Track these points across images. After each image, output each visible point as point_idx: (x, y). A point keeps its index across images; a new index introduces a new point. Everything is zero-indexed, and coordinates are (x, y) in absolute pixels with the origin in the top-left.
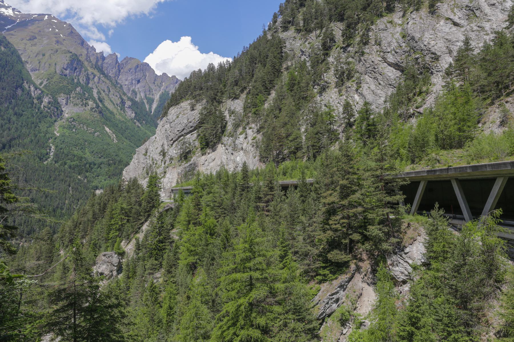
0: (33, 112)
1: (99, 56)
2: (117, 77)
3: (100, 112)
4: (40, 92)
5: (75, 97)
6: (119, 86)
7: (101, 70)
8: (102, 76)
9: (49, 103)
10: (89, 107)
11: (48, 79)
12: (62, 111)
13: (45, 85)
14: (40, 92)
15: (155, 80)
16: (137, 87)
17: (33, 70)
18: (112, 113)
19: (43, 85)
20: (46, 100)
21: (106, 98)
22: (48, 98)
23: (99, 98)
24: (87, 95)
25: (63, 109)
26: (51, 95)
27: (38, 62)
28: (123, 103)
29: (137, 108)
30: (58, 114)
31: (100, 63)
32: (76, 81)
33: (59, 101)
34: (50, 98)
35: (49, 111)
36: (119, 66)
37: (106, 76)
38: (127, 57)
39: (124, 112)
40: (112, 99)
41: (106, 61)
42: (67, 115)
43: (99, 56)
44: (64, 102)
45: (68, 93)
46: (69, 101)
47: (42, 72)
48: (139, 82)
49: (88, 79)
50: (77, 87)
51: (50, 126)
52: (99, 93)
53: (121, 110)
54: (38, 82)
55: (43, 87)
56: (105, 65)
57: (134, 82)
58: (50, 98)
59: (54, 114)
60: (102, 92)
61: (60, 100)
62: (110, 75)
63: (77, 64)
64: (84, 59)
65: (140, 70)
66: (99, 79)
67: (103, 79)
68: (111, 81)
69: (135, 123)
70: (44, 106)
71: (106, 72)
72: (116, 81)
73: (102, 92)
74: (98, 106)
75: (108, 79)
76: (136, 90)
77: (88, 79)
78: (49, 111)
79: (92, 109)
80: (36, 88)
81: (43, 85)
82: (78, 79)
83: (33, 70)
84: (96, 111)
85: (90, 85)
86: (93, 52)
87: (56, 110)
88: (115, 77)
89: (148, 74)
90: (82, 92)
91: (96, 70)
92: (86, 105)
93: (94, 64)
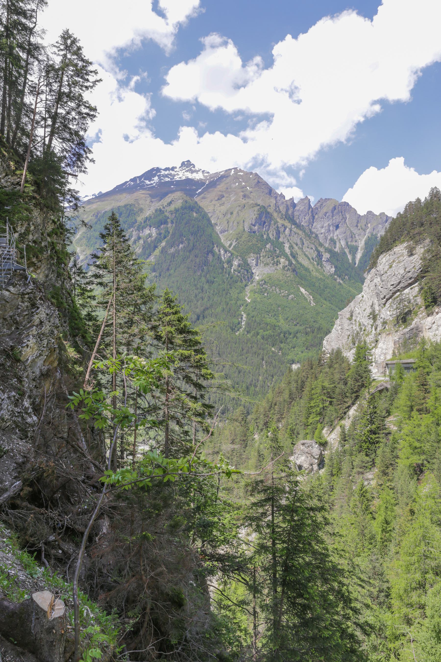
0: (224, 278)
1: (289, 203)
2: (310, 226)
3: (294, 270)
4: (229, 254)
5: (265, 255)
6: (314, 235)
7: (292, 220)
8: (293, 226)
9: (239, 265)
10: (281, 266)
11: (237, 239)
12: (253, 273)
13: (234, 247)
14: (229, 254)
15: (358, 222)
16: (335, 234)
17: (223, 231)
18: (307, 270)
19: (232, 247)
20: (236, 263)
21: (299, 252)
22: (237, 260)
23: (292, 254)
24: (278, 252)
25: (254, 271)
26: (240, 256)
27: (226, 222)
28: (320, 256)
29: (337, 260)
30: (248, 278)
31: (290, 212)
32: (265, 237)
33: (249, 262)
34: (239, 260)
35: (239, 274)
36: (312, 211)
37: (298, 226)
38: (321, 199)
39: (322, 268)
40: (307, 253)
41: (297, 208)
42: (257, 278)
43: (289, 203)
44: (254, 262)
45: (258, 252)
46: (259, 261)
47: (231, 232)
48: (337, 227)
49: (278, 233)
50: (267, 244)
51: (241, 292)
52: (291, 247)
53: (318, 265)
54: (227, 244)
55: (232, 249)
56: (296, 213)
57: (331, 228)
58: (239, 260)
59: (244, 277)
60: (295, 246)
61: (249, 260)
62: (302, 224)
63: (266, 217)
64: (272, 210)
65: (338, 213)
66: (291, 231)
67: (295, 230)
68: (304, 232)
69: (335, 280)
70: (234, 270)
71: (297, 222)
72: (310, 230)
73: (295, 246)
74: (291, 264)
75: (301, 230)
76: (335, 238)
77: (278, 233)
79: (284, 267)
80: (226, 251)
81: (232, 247)
82: (268, 234)
83: (223, 231)
84: (289, 269)
85: (281, 240)
86: (282, 199)
87: (246, 273)
88: (308, 225)
89: (348, 216)
90: (272, 248)
91: (287, 221)
92: (278, 263)
93: (284, 214)
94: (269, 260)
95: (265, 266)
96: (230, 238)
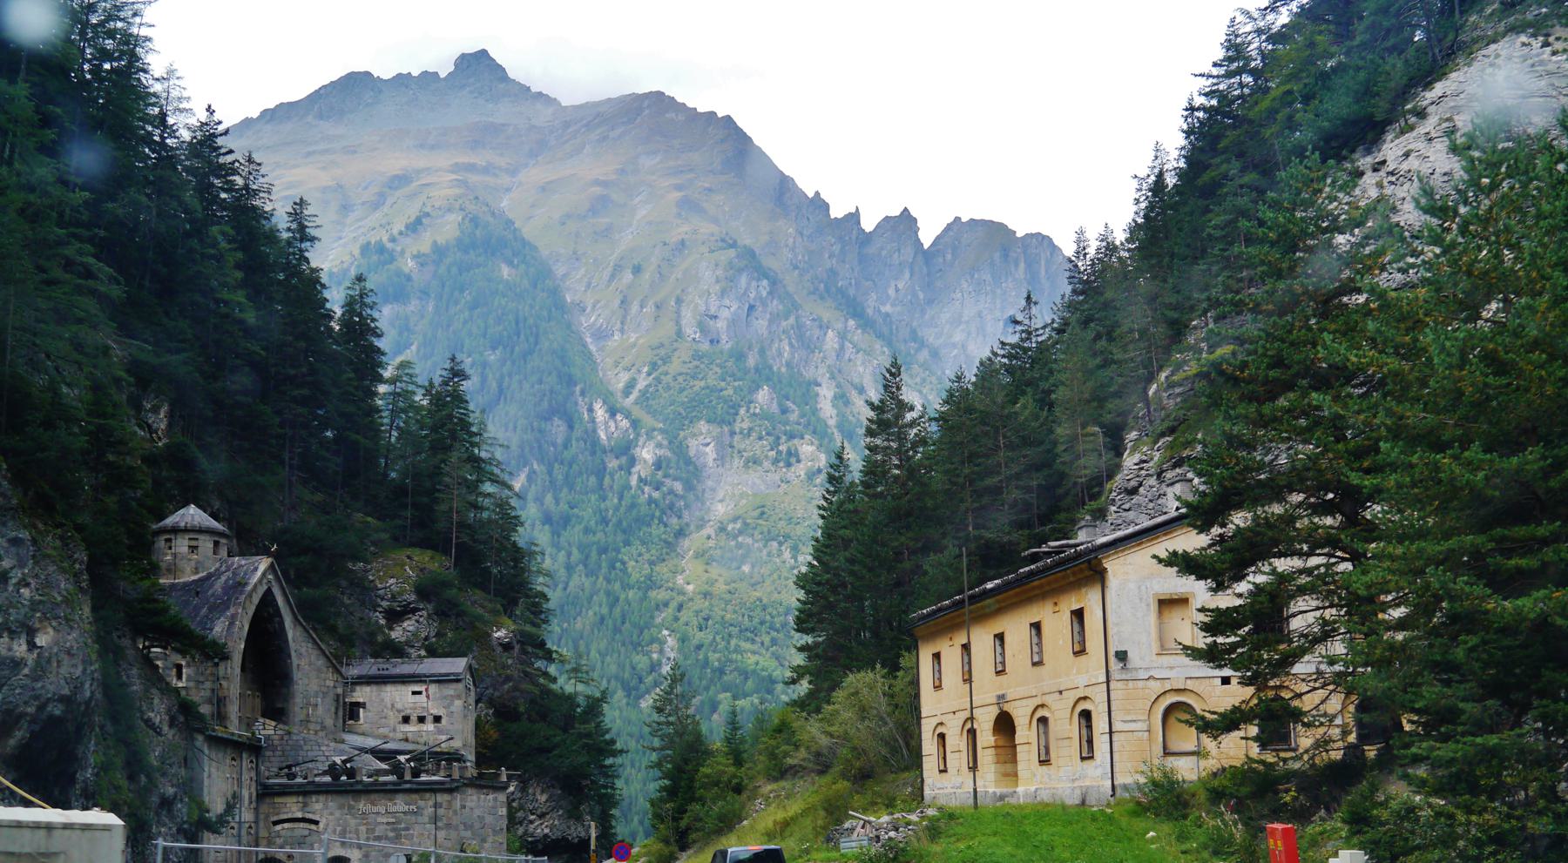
5: (750, 429)
8: (851, 323)
9: (658, 465)
11: (654, 366)
13: (644, 393)
22: (651, 445)
26: (662, 431)
27: (617, 302)
32: (751, 361)
33: (692, 453)
35: (656, 495)
42: (720, 510)
50: (758, 387)
55: (636, 403)
58: (659, 445)
61: (693, 445)
66: (842, 336)
67: (858, 336)
70: (640, 480)
78: (656, 495)
80: (612, 412)
92: (792, 457)
94: (760, 447)
95: (746, 466)
96: (626, 362)
